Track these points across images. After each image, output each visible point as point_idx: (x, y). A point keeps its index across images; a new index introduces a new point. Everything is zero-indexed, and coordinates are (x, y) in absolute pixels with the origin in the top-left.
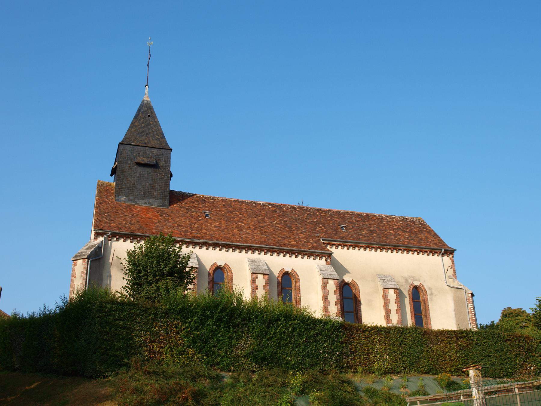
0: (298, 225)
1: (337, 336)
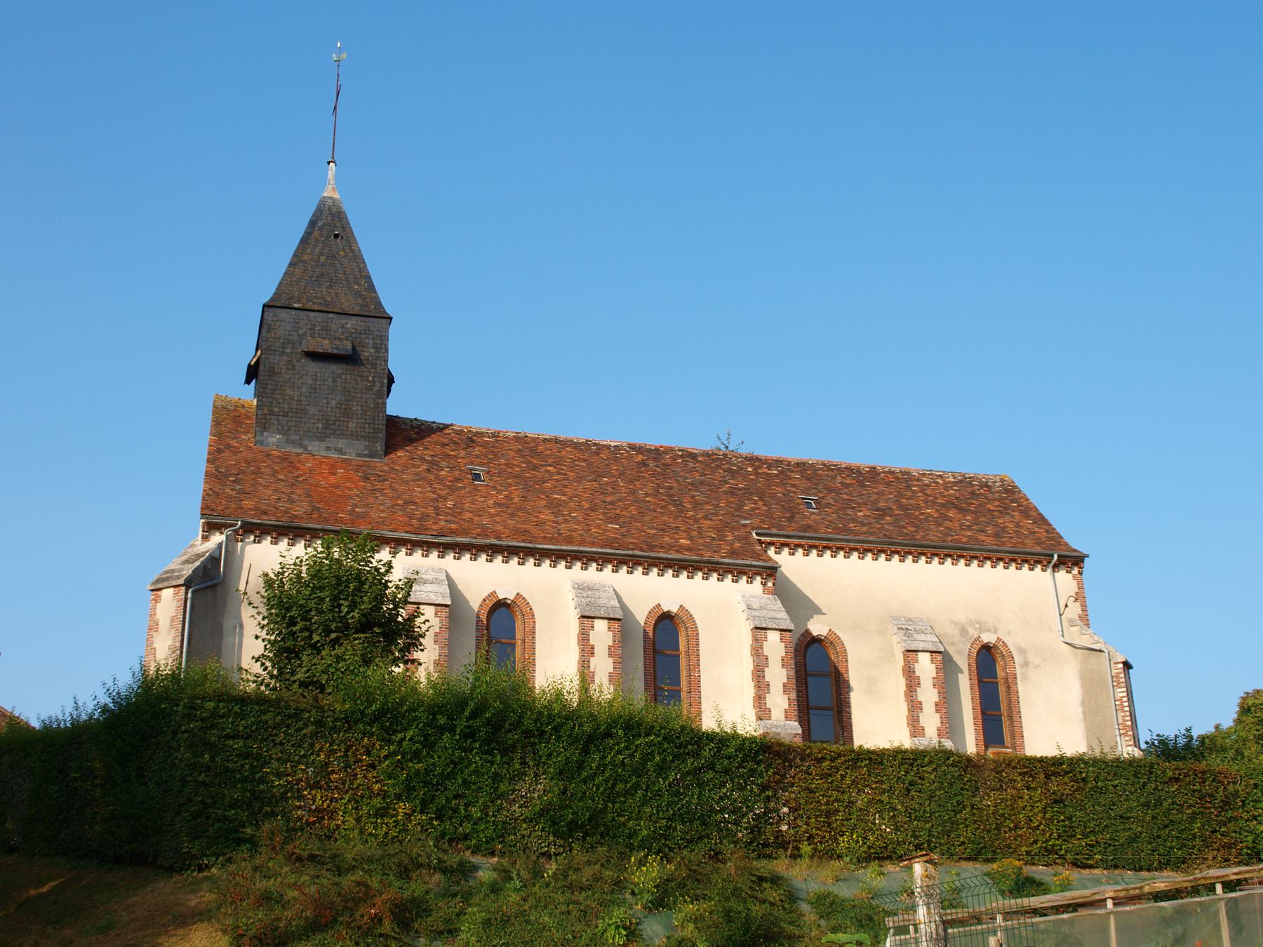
0: (700, 497)
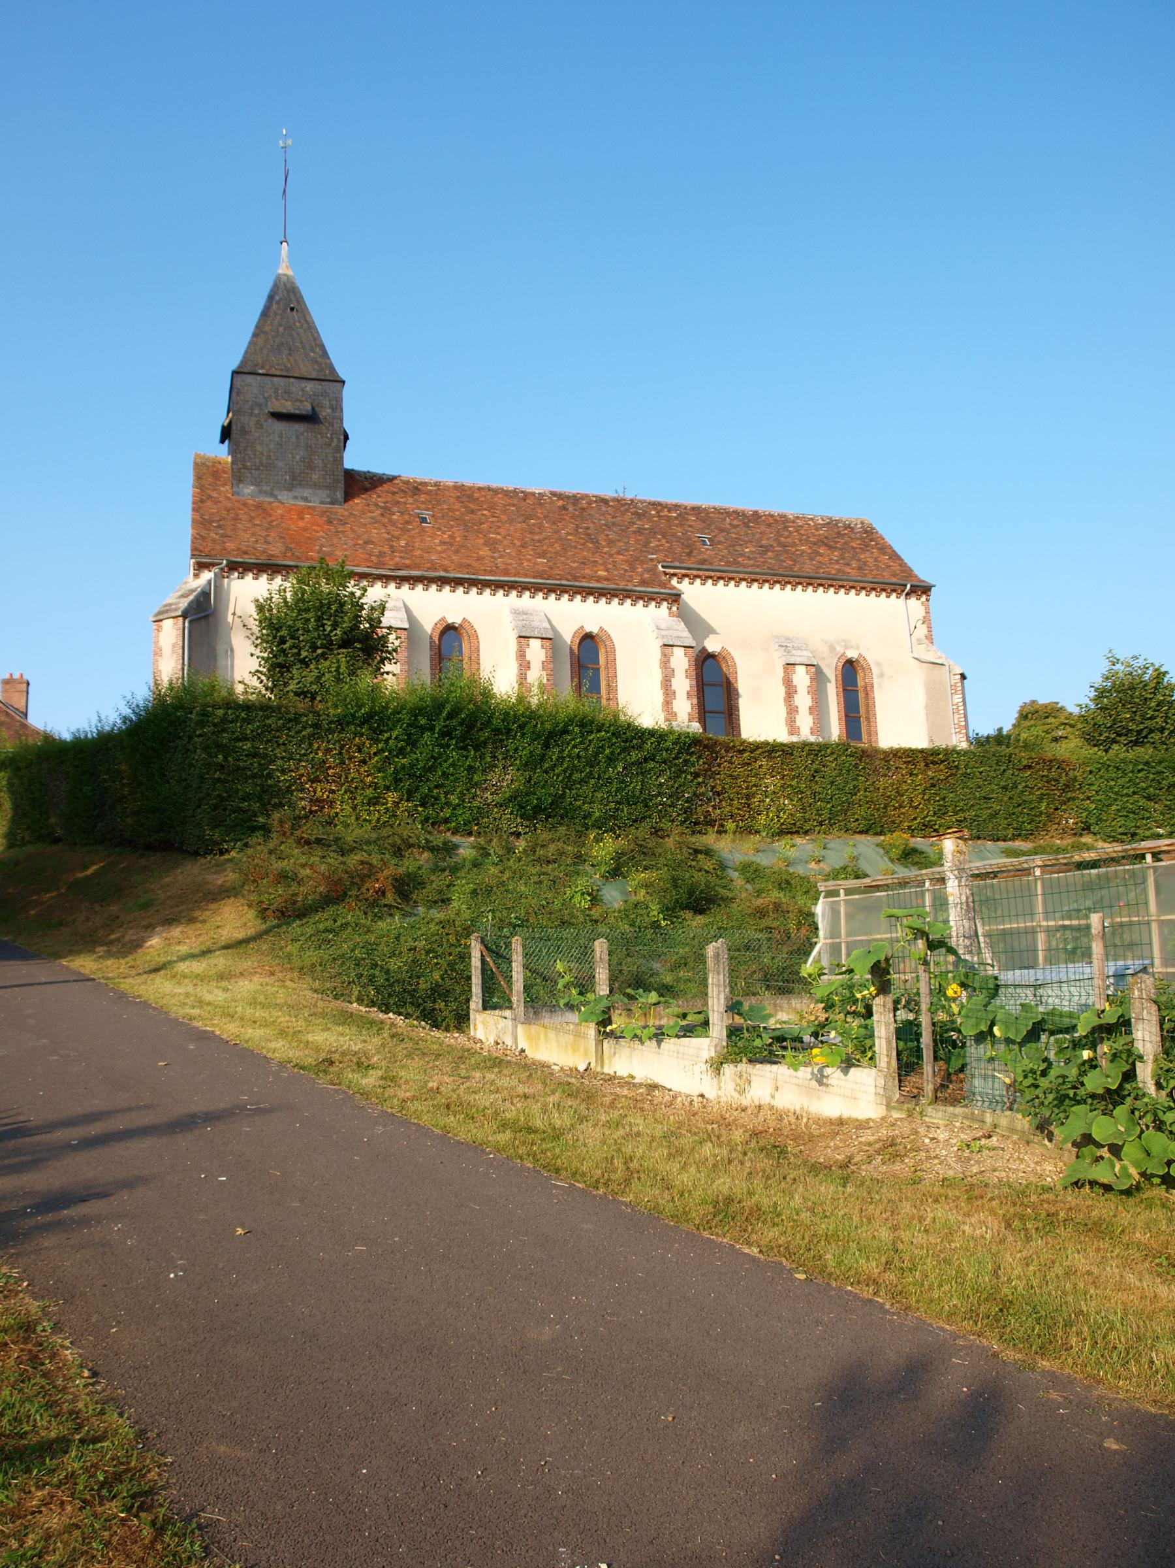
0: (612, 536)
1: (685, 761)
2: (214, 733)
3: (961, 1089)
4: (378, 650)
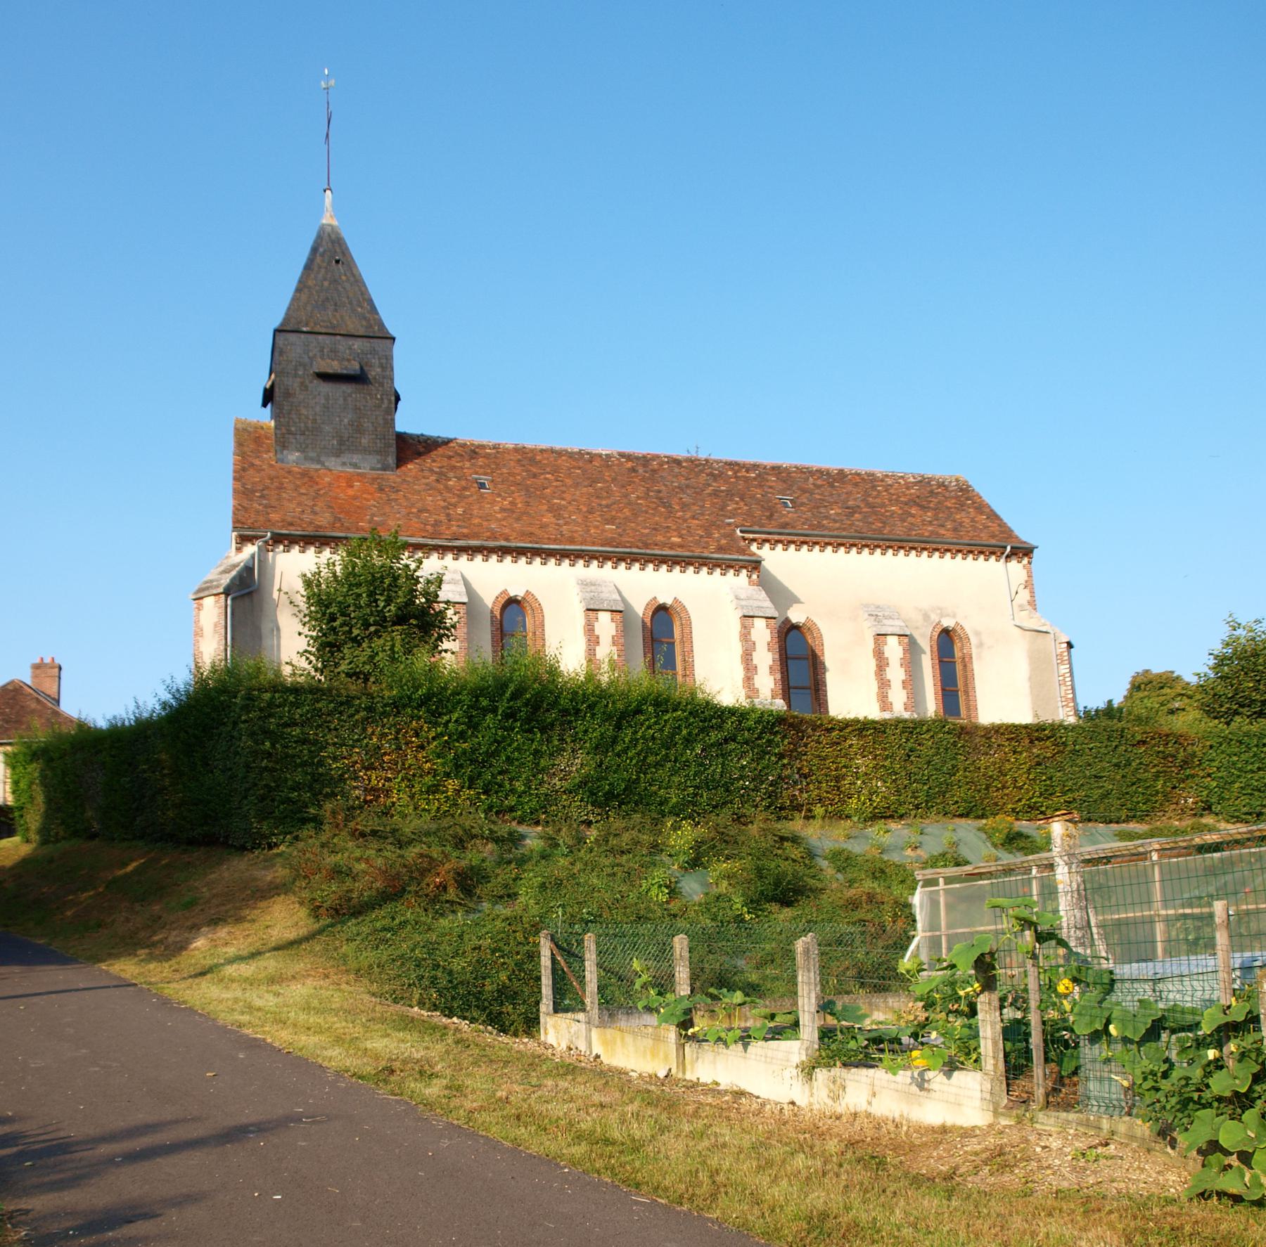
0: (686, 499)
1: (768, 741)
2: (260, 718)
3: (1075, 1093)
4: (435, 626)
